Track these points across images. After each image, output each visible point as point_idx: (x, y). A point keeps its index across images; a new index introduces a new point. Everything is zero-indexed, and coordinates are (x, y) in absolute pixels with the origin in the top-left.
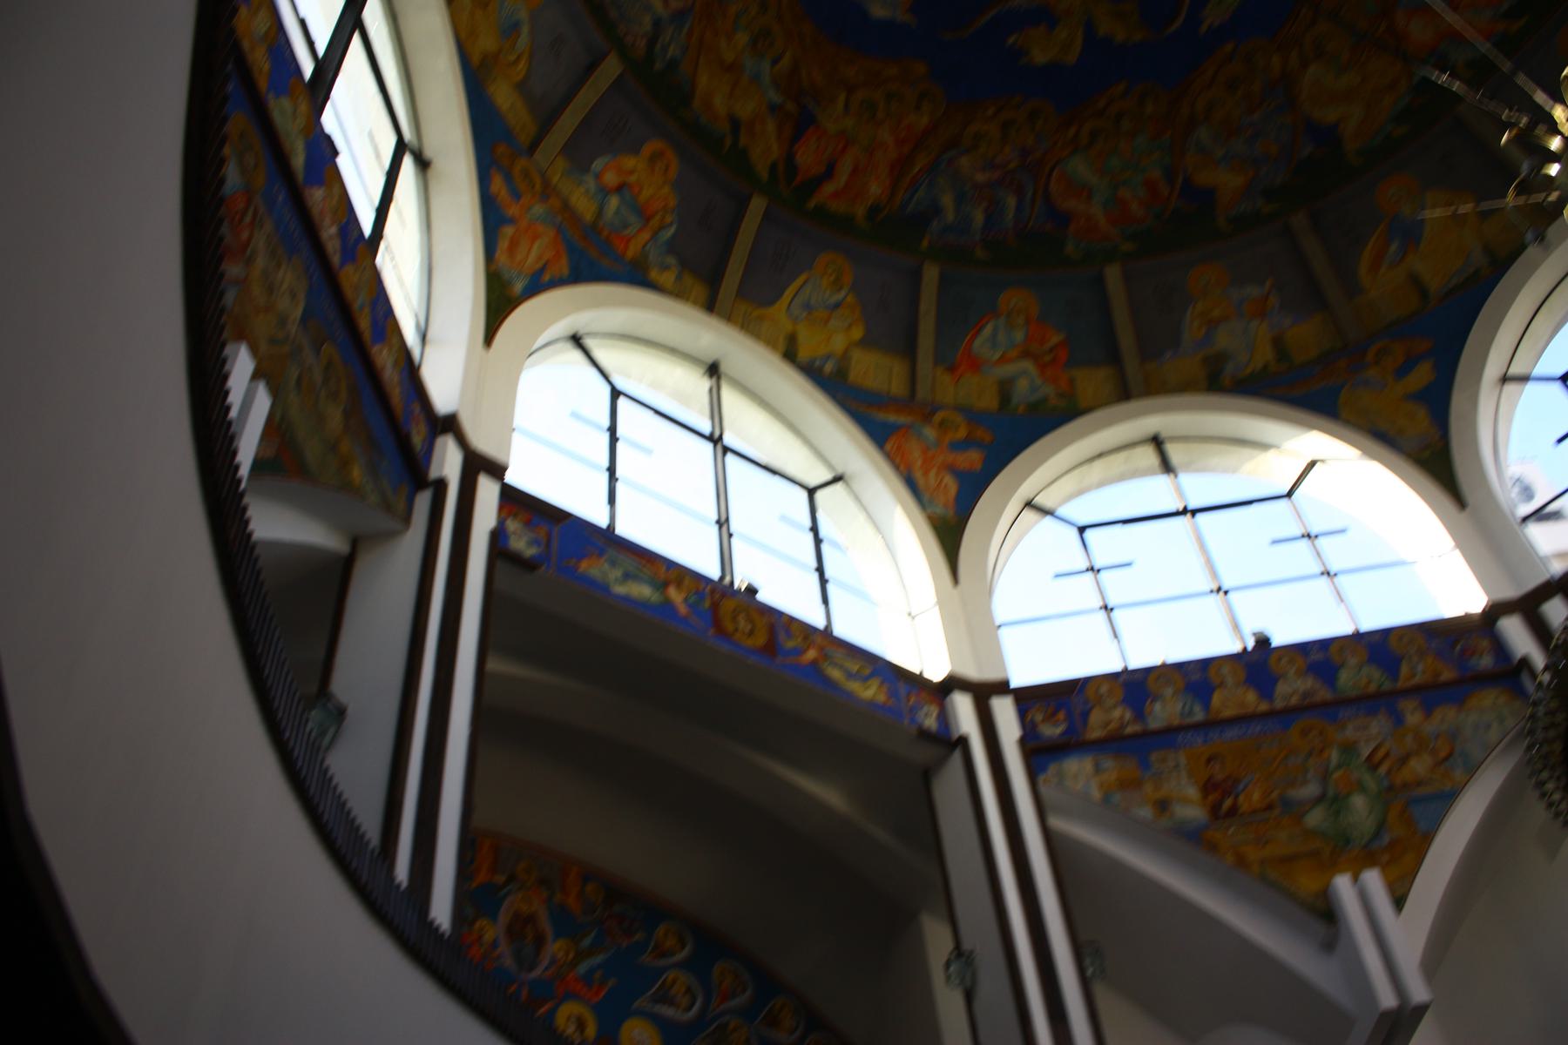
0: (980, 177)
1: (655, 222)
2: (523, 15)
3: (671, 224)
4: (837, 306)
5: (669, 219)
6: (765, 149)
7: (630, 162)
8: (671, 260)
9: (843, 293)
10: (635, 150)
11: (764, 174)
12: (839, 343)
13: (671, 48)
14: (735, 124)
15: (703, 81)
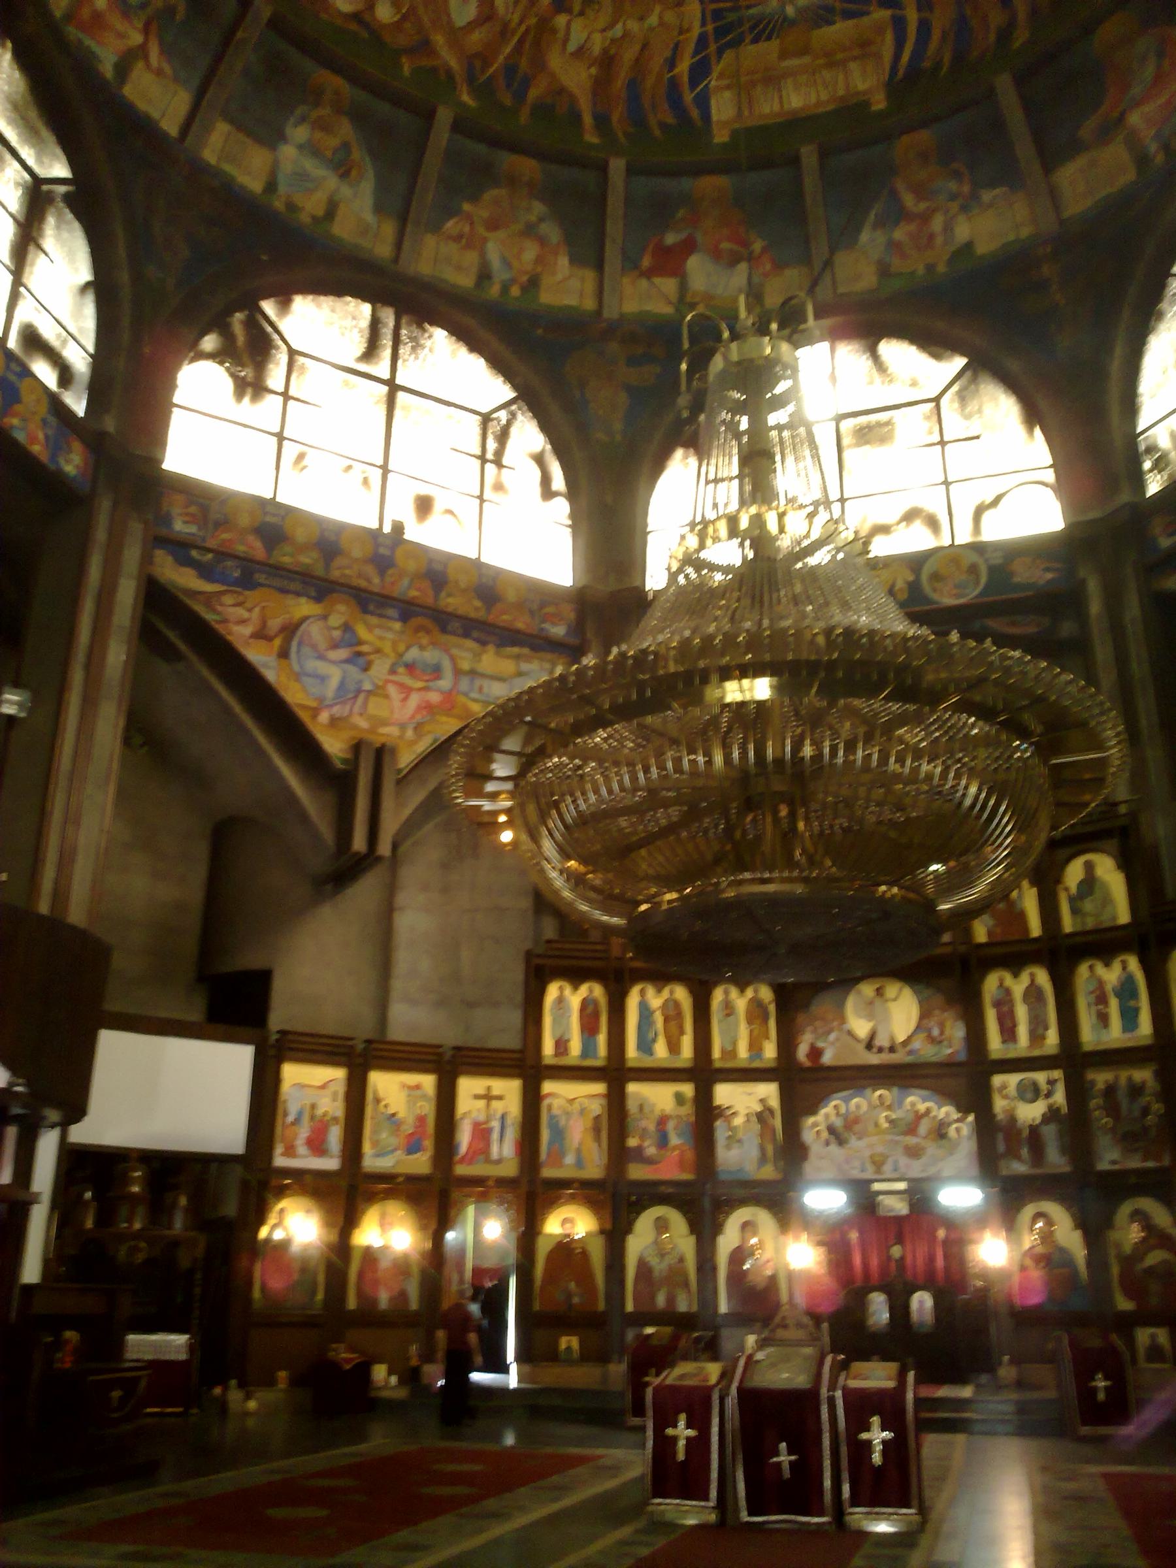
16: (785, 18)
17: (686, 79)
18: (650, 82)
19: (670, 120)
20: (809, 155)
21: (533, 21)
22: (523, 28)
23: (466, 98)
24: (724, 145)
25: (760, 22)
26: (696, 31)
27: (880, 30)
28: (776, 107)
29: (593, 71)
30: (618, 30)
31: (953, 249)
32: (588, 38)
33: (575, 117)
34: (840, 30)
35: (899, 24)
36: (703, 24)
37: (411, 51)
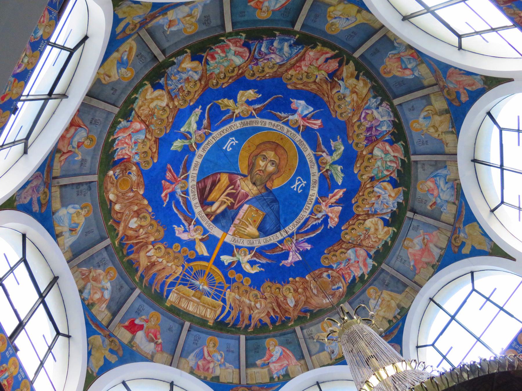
0: (273, 56)
1: (396, 56)
2: (421, 120)
3: (390, 54)
4: (335, 18)
5: (390, 56)
6: (349, 69)
7: (398, 74)
8: (396, 44)
9: (331, 22)
10: (395, 77)
11: (351, 61)
12: (341, 7)
13: (373, 102)
14: (357, 78)
15: (365, 91)
16: (199, 288)
17: (168, 284)
18: (160, 277)
19: (158, 291)
20: (187, 324)
21: (145, 241)
22: (141, 240)
23: (116, 243)
24: (168, 306)
25: (193, 284)
26: (178, 275)
27: (219, 306)
28: (185, 307)
29: (149, 264)
30: (160, 260)
31: (213, 376)
32: (153, 256)
33: (137, 270)
34: (209, 299)
35: (224, 309)
36: (180, 275)
37: (115, 221)
